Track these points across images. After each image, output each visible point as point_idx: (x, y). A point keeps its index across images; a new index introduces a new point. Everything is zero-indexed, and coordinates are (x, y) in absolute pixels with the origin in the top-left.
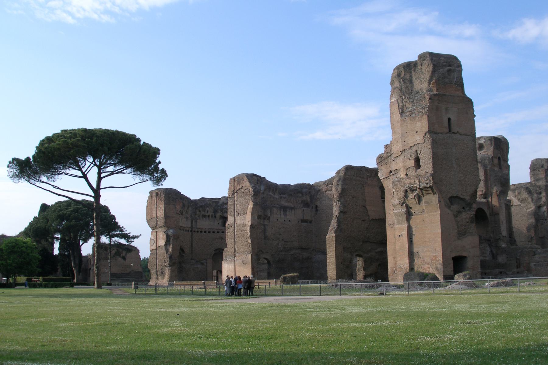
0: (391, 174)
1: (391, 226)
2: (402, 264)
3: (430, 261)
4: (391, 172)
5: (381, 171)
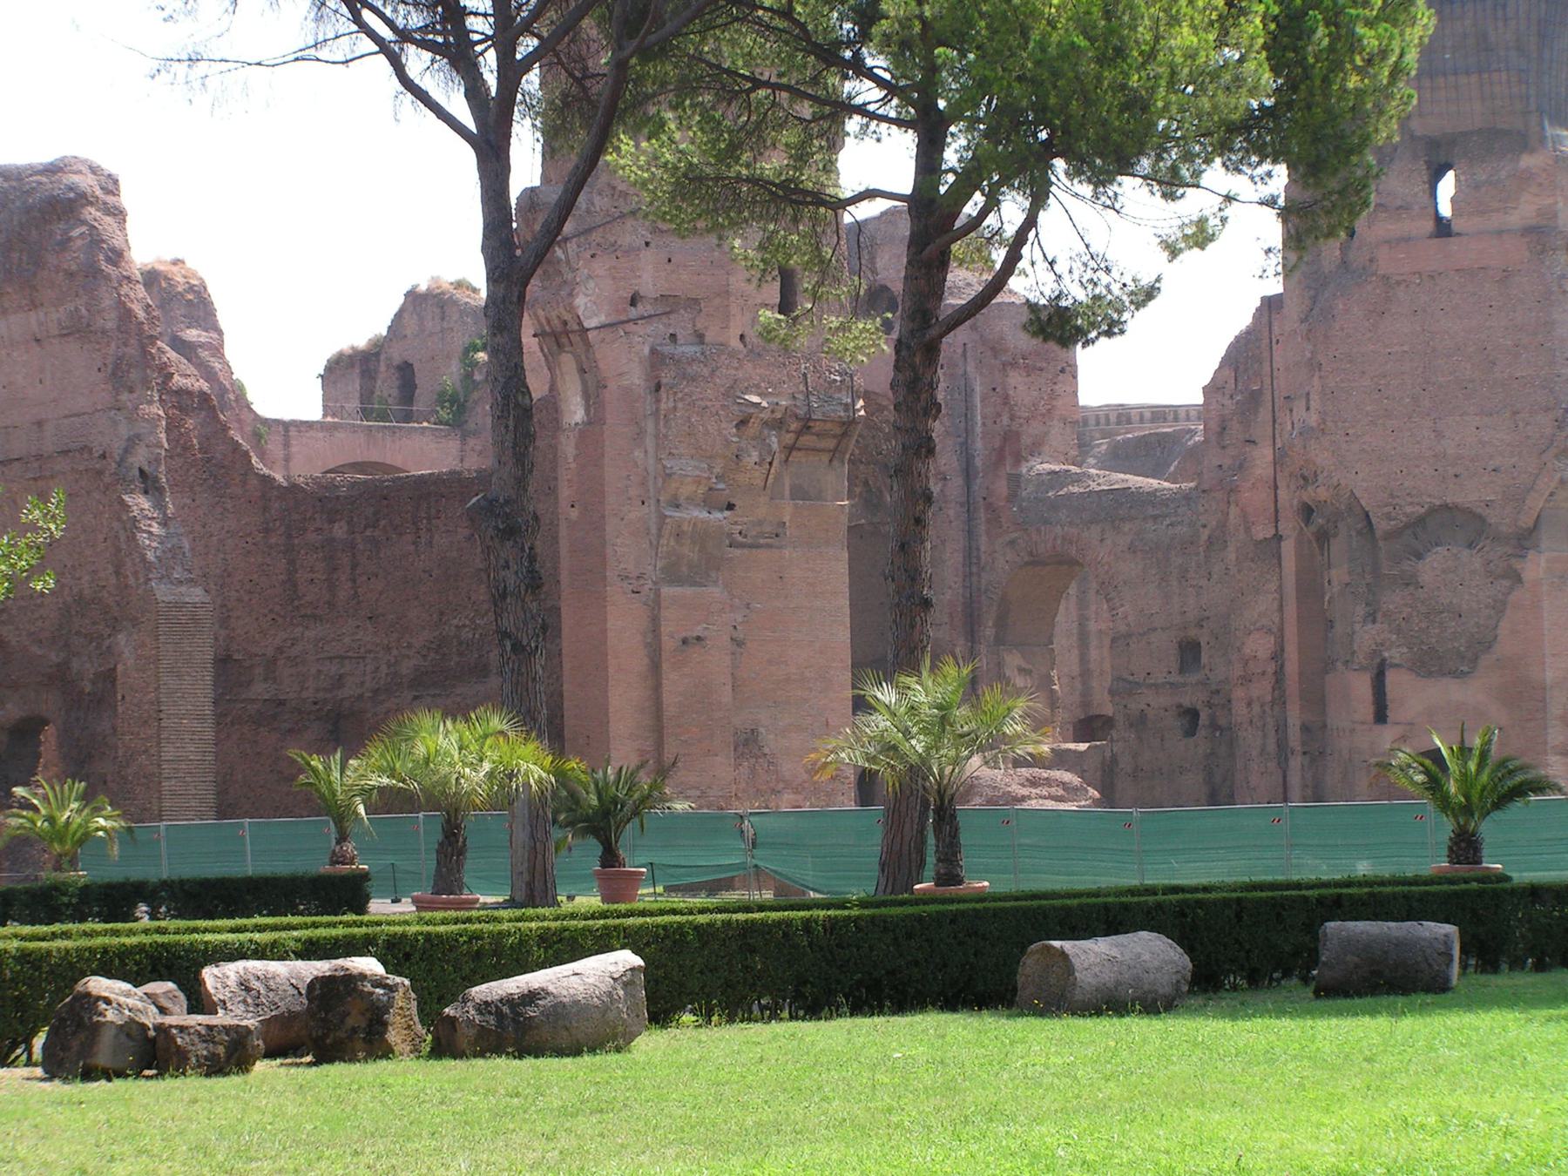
0: (634, 312)
1: (631, 587)
2: (698, 788)
3: (805, 776)
4: (633, 302)
5: (591, 284)
